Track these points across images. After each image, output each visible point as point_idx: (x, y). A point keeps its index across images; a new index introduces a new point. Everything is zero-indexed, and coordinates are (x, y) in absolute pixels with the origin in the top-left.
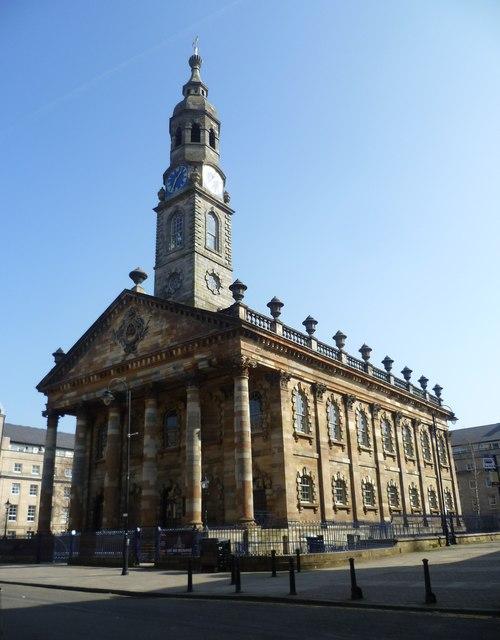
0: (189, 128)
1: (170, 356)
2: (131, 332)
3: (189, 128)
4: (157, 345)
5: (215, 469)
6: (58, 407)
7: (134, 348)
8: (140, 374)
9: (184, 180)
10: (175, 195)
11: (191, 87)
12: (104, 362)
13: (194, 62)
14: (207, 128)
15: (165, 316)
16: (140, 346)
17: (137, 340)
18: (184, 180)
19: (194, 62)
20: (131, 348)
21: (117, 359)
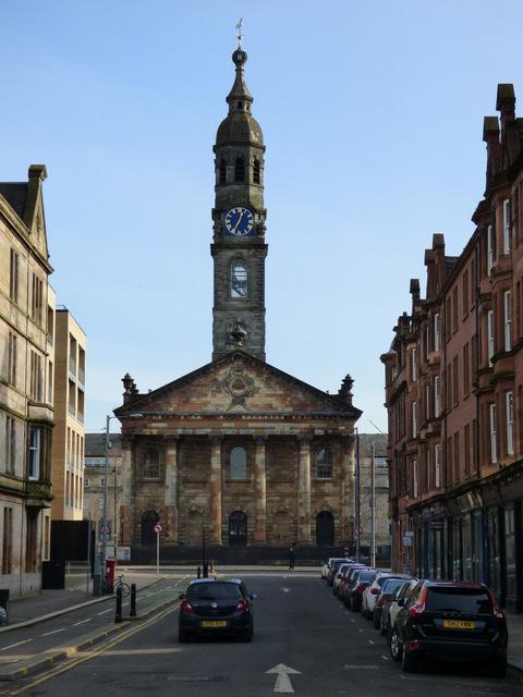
0: (237, 155)
1: (288, 419)
2: (238, 386)
3: (237, 155)
4: (270, 406)
5: (287, 501)
6: (147, 432)
7: (242, 402)
8: (250, 425)
9: (250, 227)
10: (235, 241)
11: (238, 99)
12: (205, 404)
13: (239, 58)
14: (252, 160)
15: (277, 383)
16: (248, 401)
17: (246, 395)
18: (250, 227)
19: (239, 58)
20: (238, 400)
21: (221, 406)
